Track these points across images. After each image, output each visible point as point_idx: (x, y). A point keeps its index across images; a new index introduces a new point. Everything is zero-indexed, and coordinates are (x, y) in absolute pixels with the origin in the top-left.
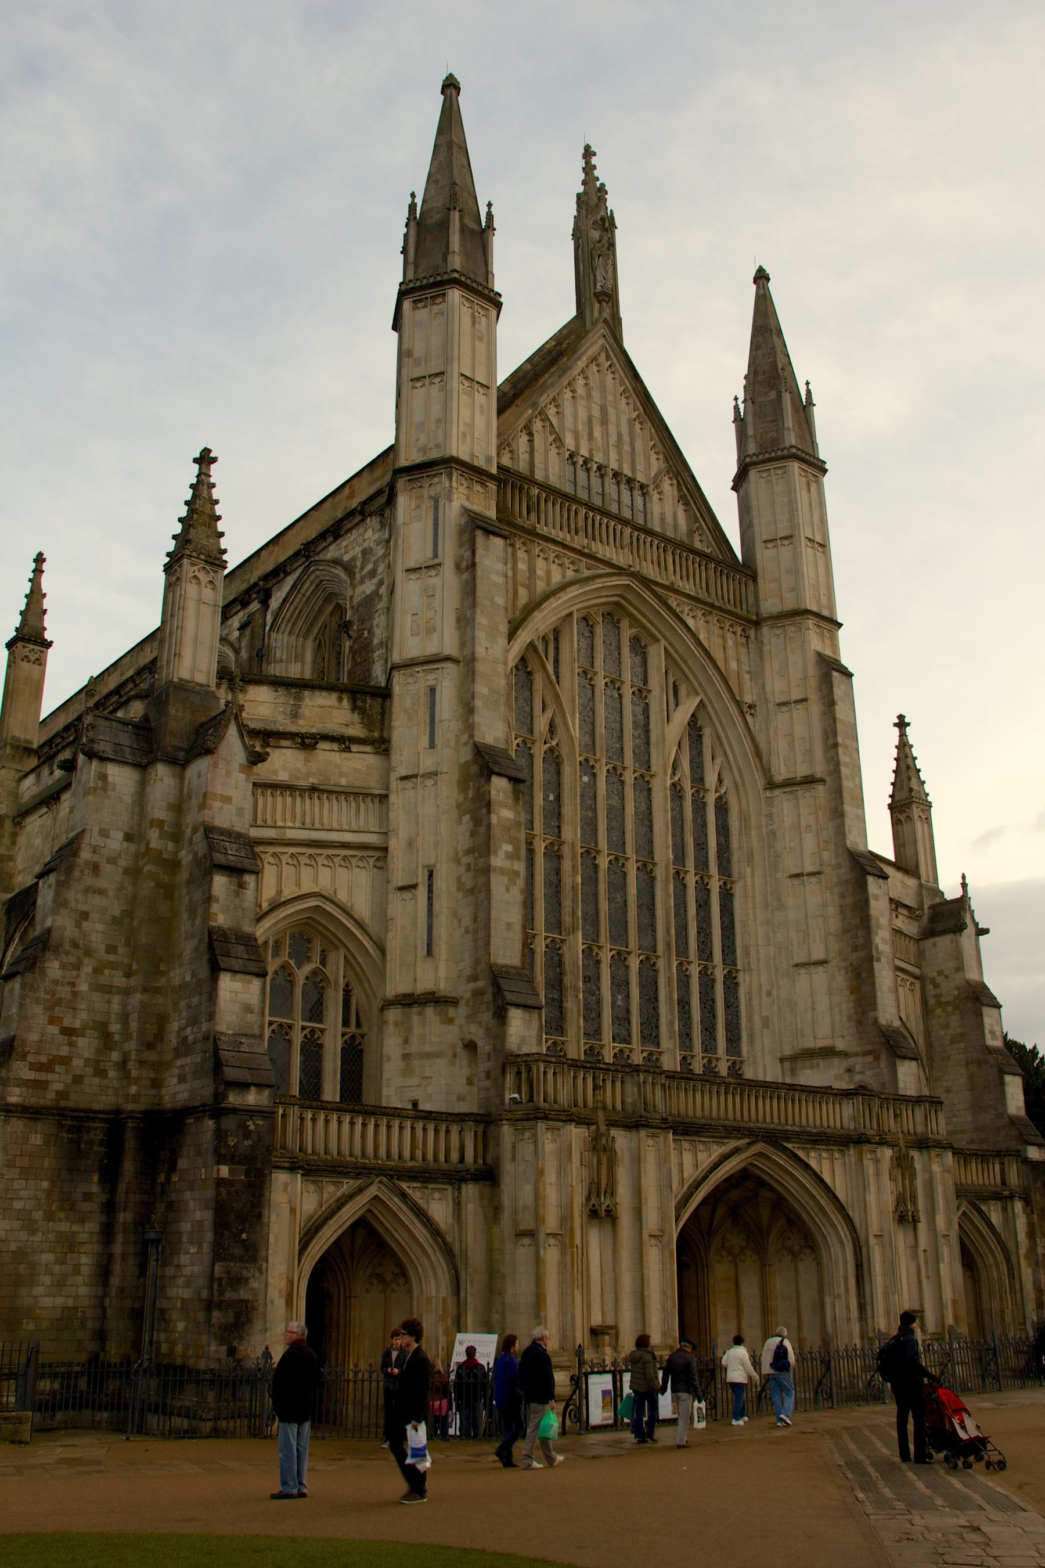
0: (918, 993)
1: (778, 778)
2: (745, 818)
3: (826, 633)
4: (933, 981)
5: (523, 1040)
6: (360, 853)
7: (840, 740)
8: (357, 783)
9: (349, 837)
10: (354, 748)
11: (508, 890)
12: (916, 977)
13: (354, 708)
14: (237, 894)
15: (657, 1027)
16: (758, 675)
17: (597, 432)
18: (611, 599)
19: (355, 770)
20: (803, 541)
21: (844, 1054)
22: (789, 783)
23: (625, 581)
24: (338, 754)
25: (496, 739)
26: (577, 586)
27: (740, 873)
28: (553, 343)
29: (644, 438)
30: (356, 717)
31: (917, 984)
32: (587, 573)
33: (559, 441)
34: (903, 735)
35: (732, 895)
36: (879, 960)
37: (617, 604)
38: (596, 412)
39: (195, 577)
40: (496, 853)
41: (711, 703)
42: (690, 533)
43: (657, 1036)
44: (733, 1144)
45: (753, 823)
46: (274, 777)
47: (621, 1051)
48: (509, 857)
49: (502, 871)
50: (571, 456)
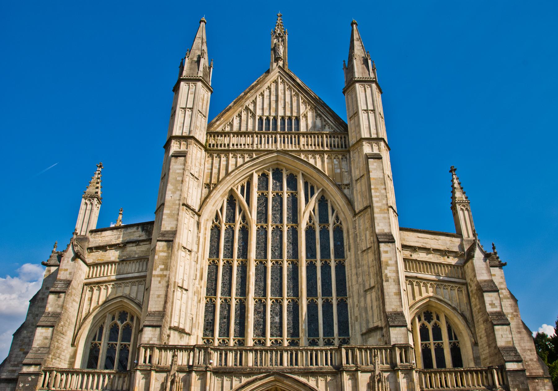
0: (464, 292)
1: (357, 211)
2: (348, 232)
3: (374, 144)
4: (469, 283)
5: (151, 339)
7: (372, 187)
8: (142, 255)
10: (141, 244)
11: (160, 282)
12: (463, 284)
13: (143, 230)
14: (57, 300)
16: (350, 172)
17: (273, 105)
18: (273, 163)
19: (142, 251)
20: (360, 112)
21: (381, 328)
22: (360, 211)
23: (275, 155)
24: (135, 247)
25: (172, 228)
26: (249, 163)
27: (347, 255)
30: (144, 233)
31: (464, 288)
32: (254, 156)
33: (254, 116)
35: (344, 266)
36: (387, 281)
37: (277, 164)
38: (273, 98)
39: (86, 204)
40: (155, 270)
42: (323, 127)
44: (255, 377)
45: (350, 233)
46: (109, 260)
48: (162, 270)
49: (158, 276)
50: (261, 119)
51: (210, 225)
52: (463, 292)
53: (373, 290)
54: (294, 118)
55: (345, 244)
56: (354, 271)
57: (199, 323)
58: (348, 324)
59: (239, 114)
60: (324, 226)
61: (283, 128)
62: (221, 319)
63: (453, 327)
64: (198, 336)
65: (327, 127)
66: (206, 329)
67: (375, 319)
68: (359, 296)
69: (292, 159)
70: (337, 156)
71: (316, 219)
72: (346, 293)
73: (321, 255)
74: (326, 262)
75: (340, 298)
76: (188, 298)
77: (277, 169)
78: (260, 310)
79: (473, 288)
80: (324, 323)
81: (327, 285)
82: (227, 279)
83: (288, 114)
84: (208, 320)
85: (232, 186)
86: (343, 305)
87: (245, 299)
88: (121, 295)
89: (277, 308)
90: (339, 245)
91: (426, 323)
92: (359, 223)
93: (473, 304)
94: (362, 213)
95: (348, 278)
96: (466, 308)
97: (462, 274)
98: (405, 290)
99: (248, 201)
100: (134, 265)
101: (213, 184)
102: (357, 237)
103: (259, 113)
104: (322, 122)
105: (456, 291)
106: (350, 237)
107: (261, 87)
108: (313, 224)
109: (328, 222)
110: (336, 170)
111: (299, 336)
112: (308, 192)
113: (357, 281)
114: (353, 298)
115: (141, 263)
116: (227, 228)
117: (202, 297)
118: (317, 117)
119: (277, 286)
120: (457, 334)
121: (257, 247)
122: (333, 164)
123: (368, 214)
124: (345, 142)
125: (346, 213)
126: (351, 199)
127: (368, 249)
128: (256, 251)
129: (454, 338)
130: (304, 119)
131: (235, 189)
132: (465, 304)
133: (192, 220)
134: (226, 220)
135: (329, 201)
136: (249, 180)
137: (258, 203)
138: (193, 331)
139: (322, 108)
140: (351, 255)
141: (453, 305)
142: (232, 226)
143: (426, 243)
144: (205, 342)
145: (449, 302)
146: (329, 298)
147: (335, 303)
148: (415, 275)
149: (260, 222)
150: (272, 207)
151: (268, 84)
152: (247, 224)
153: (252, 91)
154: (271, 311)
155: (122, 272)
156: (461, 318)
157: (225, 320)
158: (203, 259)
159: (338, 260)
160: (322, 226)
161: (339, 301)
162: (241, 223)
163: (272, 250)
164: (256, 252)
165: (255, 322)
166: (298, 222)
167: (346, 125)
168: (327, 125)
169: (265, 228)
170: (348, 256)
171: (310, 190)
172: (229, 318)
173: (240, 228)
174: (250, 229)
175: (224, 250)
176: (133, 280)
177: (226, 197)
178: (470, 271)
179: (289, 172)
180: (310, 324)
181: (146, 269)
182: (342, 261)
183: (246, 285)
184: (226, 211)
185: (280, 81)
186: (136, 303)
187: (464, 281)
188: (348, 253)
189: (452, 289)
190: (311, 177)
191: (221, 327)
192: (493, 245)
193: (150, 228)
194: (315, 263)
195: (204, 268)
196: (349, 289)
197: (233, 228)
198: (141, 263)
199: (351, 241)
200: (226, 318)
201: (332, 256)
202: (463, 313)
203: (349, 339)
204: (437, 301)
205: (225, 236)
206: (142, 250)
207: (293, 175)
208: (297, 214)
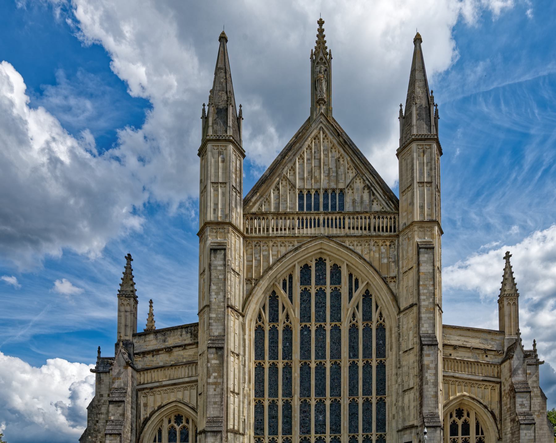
0: (497, 391)
2: (391, 330)
6: (191, 384)
9: (187, 380)
15: (340, 425)
28: (294, 139)
29: (346, 162)
34: (508, 262)
35: (385, 366)
37: (321, 253)
41: (372, 283)
43: (340, 429)
45: (393, 332)
47: (320, 437)
50: (301, 192)
51: (253, 325)
52: (496, 390)
53: (412, 391)
54: (338, 192)
55: (387, 343)
56: (394, 372)
57: (250, 423)
58: (385, 421)
59: (276, 187)
60: (367, 324)
61: (326, 206)
62: (269, 418)
63: (481, 424)
64: (250, 435)
65: (375, 203)
66: (256, 428)
67: (412, 417)
68: (397, 396)
69: (337, 247)
70: (384, 242)
71: (359, 315)
72: (385, 392)
73: (363, 354)
74: (367, 362)
75: (379, 397)
76: (239, 401)
77: (321, 259)
78: (305, 410)
79: (506, 388)
80: (363, 421)
81: (367, 385)
82: (273, 381)
83: (333, 185)
84: (258, 420)
85: (273, 281)
86: (381, 404)
87: (291, 400)
88: (175, 399)
89: (321, 407)
90: (381, 344)
91: (457, 419)
92: (403, 322)
93: (503, 403)
94: (407, 311)
95: (388, 378)
96: (496, 406)
97: (498, 373)
98: (441, 390)
99: (291, 297)
100: (183, 370)
101: (254, 279)
102: (399, 337)
103: (298, 184)
104: (370, 196)
105: (489, 390)
106: (393, 336)
107: (301, 147)
108: (357, 322)
109: (371, 320)
110: (382, 259)
111: (340, 433)
112: (352, 285)
113: (397, 381)
114: (392, 397)
115: (190, 368)
116: (270, 328)
117: (251, 399)
118: (364, 189)
119: (321, 387)
120: (484, 430)
121: (301, 348)
122: (380, 253)
123: (413, 313)
124: (395, 222)
125: (390, 309)
126: (396, 294)
127: (410, 349)
128: (301, 351)
129: (480, 433)
130: (350, 191)
131: (277, 283)
132: (496, 403)
133: (237, 321)
134: (270, 319)
135: (373, 296)
136: (292, 272)
137: (300, 299)
138: (246, 431)
139: (371, 177)
140: (392, 354)
141: (484, 404)
142: (276, 326)
143: (467, 342)
144: (256, 440)
145: (481, 401)
146: (368, 397)
147: (374, 401)
148: (452, 374)
149: (304, 321)
150: (316, 304)
151: (307, 143)
152: (290, 323)
153: (290, 154)
154: (315, 410)
155: (172, 377)
156: (491, 415)
157: (273, 420)
158: (250, 362)
159: (379, 359)
160: (365, 324)
161: (378, 400)
162: (284, 323)
163: (316, 351)
164: (301, 353)
165: (300, 421)
166: (342, 320)
167: (398, 201)
168: (375, 201)
169: (309, 327)
170: (389, 355)
171: (354, 283)
172: (276, 417)
173: (284, 327)
174: (294, 329)
175: (270, 351)
176: (185, 385)
177: (269, 293)
178: (506, 371)
179: (332, 263)
180: (351, 422)
181: (196, 374)
182: (383, 360)
183: (291, 385)
184: (269, 309)
185: (322, 136)
186: (190, 407)
187: (498, 380)
188: (390, 353)
189: (486, 387)
190: (356, 269)
191: (270, 426)
192: (534, 341)
193: (194, 331)
194: (357, 363)
195: (251, 370)
196: (389, 389)
197: (277, 328)
198: (190, 368)
199: (394, 340)
200: (273, 417)
201: (374, 355)
202: (493, 411)
203: (385, 435)
204: (470, 400)
205: (269, 337)
206: (189, 354)
207: (337, 265)
208: (341, 311)
